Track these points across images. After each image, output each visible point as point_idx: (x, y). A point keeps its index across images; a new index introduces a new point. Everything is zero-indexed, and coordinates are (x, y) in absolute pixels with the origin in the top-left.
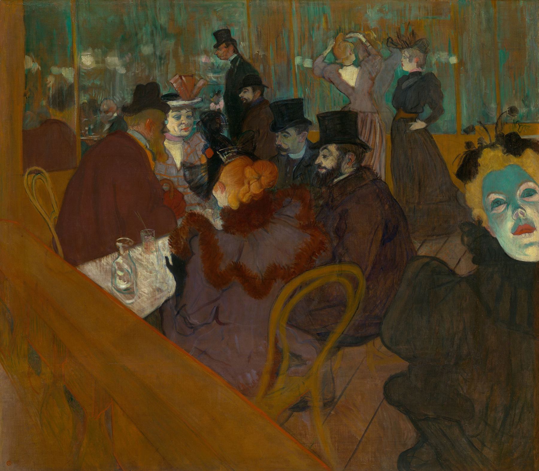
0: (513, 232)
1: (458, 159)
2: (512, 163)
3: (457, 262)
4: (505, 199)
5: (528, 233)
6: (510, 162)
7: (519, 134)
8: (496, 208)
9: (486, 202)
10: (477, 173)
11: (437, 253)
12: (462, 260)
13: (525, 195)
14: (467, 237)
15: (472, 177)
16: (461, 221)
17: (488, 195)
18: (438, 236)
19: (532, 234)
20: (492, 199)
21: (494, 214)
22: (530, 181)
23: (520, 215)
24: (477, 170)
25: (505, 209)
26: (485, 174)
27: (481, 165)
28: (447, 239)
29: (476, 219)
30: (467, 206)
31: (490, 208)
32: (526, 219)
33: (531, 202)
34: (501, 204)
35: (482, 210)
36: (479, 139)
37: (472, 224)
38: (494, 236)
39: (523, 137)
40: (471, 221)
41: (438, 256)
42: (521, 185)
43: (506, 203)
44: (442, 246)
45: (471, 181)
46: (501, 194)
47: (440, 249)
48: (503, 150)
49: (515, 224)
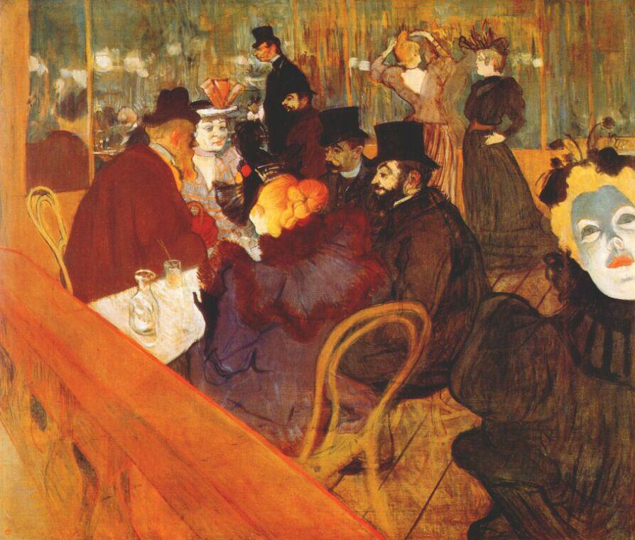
4: (598, 227)
8: (588, 237)
19: (630, 267)
20: (584, 226)
28: (529, 273)
45: (557, 205)
48: (596, 170)
49: (610, 255)
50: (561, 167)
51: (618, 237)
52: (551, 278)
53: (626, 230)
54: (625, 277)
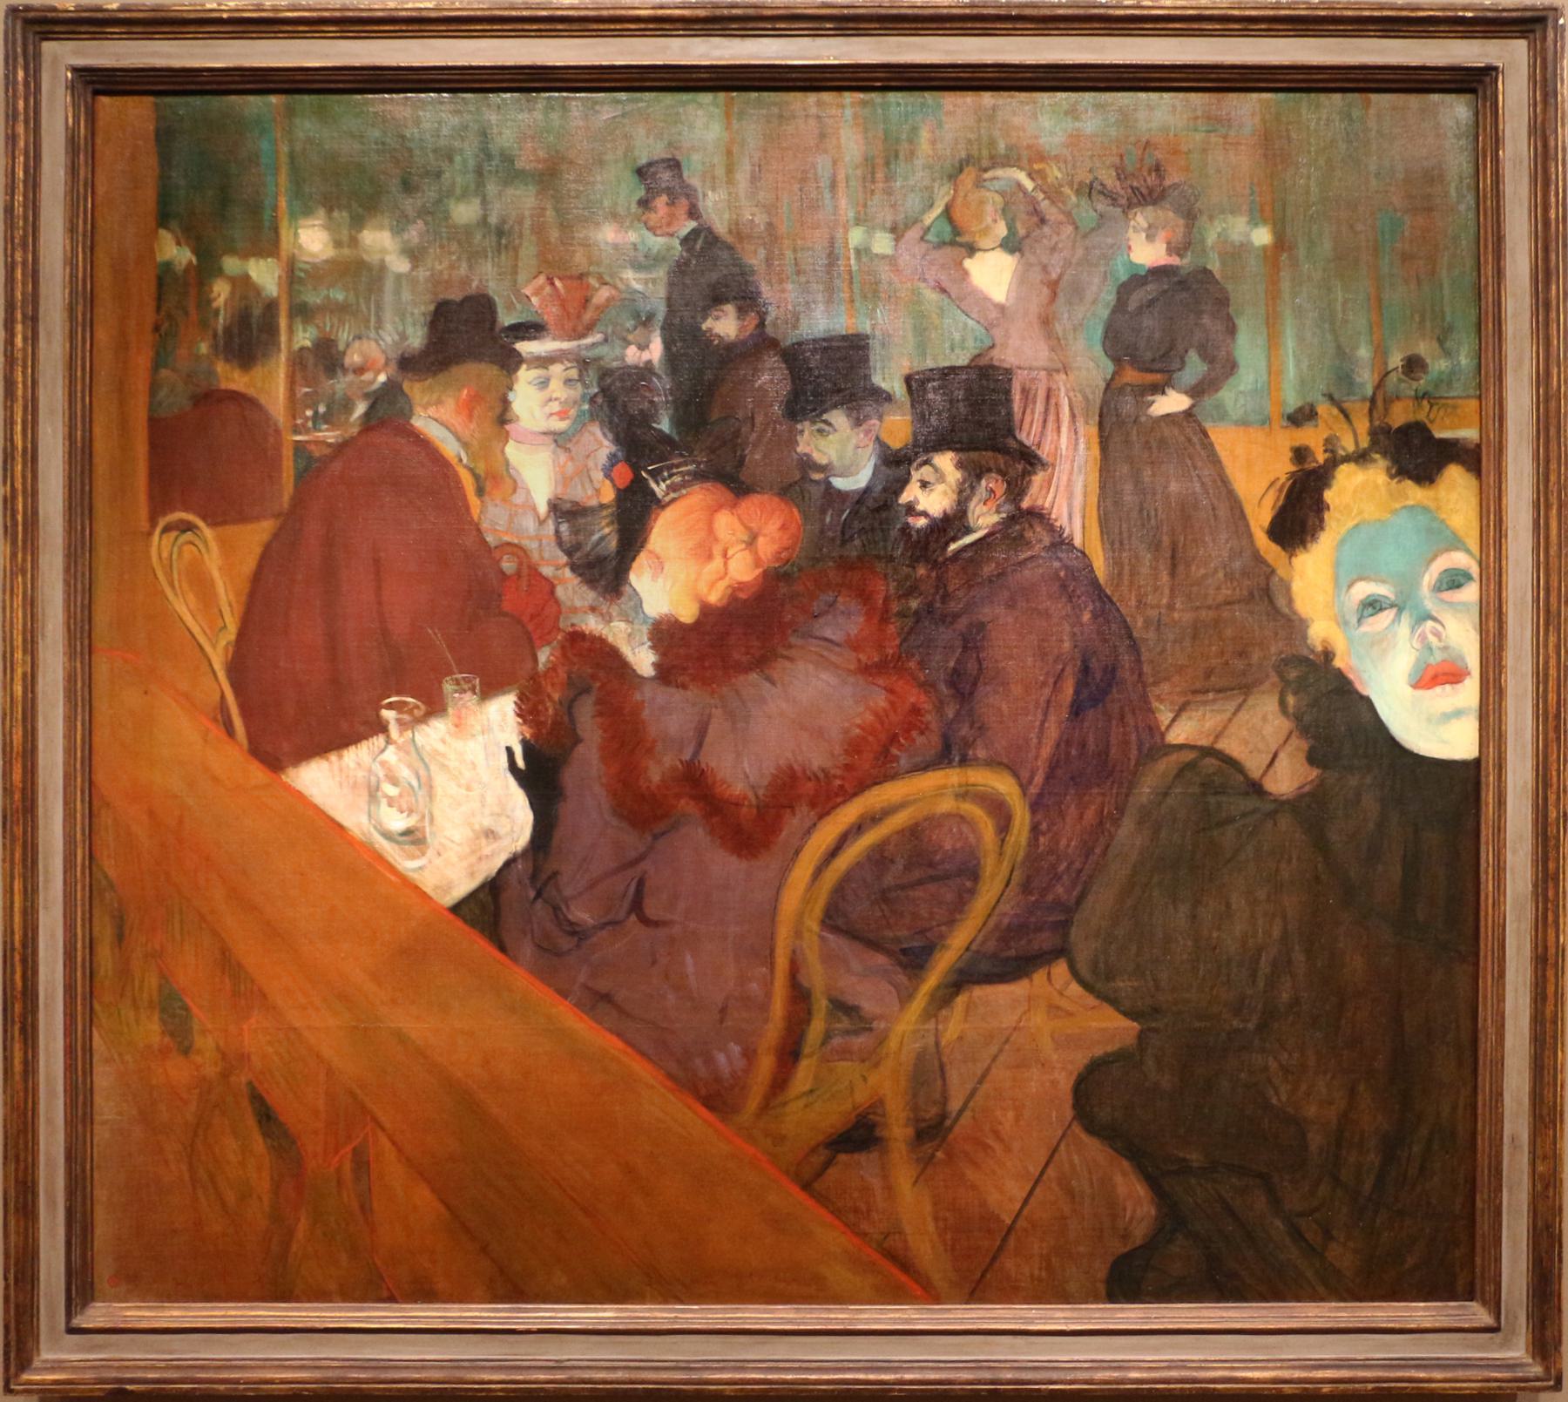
2: (1411, 502)
3: (1267, 762)
4: (1392, 597)
5: (1452, 683)
6: (1407, 498)
7: (1429, 425)
8: (1370, 620)
10: (1322, 529)
11: (1217, 737)
12: (1282, 755)
13: (1445, 586)
14: (1295, 693)
15: (1309, 538)
16: (1281, 652)
17: (1350, 586)
18: (1219, 691)
19: (1459, 686)
20: (1362, 596)
21: (1365, 634)
22: (1457, 549)
23: (1432, 639)
24: (1322, 520)
25: (1393, 621)
26: (1343, 531)
28: (1245, 701)
29: (1319, 648)
30: (1295, 613)
31: (1354, 620)
32: (1446, 648)
33: (1459, 603)
34: (1381, 609)
35: (1334, 626)
36: (1327, 441)
37: (1307, 659)
38: (1365, 693)
40: (1305, 652)
41: (1220, 746)
44: (1230, 720)
45: (1305, 547)
46: (1383, 582)
47: (1225, 728)
48: (1388, 470)
49: (1418, 660)
50: (1314, 465)
51: (1435, 619)
52: (1291, 710)
53: (1451, 604)
54: (1449, 710)
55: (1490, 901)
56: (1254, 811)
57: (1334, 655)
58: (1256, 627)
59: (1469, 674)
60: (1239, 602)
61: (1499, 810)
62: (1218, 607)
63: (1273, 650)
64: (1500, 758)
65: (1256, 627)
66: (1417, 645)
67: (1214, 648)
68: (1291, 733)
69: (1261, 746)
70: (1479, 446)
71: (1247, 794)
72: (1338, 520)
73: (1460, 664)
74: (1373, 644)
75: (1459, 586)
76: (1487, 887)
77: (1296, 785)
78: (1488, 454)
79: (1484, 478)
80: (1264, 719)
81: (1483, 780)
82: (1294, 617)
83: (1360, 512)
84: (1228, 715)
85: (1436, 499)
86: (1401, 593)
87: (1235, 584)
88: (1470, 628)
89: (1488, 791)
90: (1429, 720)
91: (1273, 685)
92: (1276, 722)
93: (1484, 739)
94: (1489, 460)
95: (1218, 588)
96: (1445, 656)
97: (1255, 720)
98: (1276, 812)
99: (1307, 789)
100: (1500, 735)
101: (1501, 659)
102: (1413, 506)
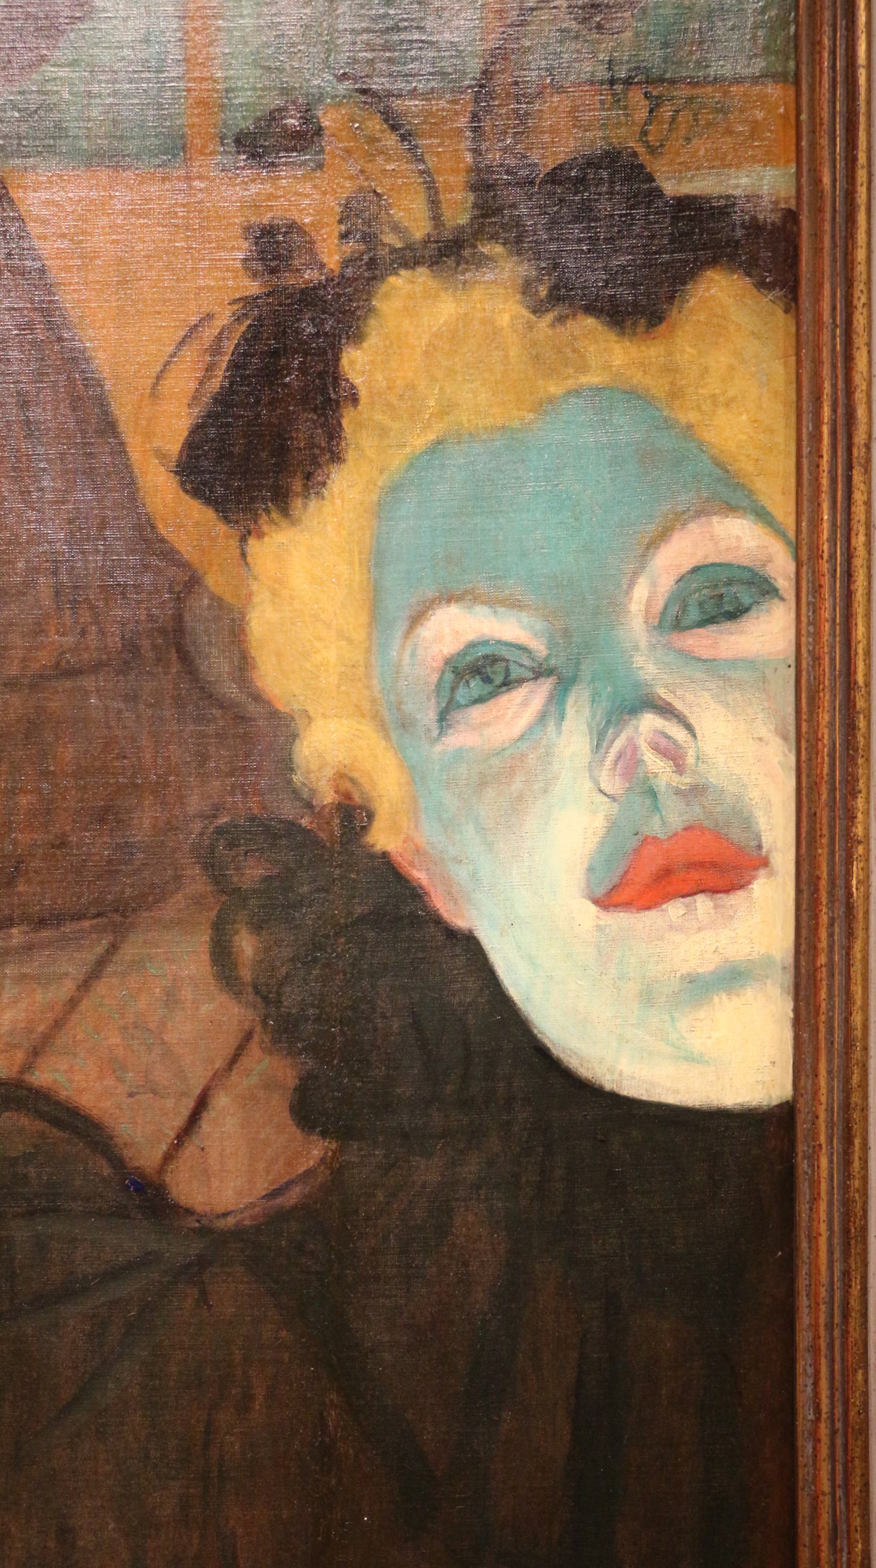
0: (600, 891)
1: (189, 354)
2: (593, 379)
3: (179, 1122)
4: (539, 647)
5: (714, 891)
6: (584, 368)
7: (644, 157)
8: (476, 713)
9: (398, 667)
10: (337, 458)
11: (36, 1052)
12: (221, 1101)
13: (694, 614)
14: (257, 927)
15: (297, 485)
16: (217, 809)
17: (417, 619)
18: (41, 923)
19: (736, 899)
20: (450, 647)
21: (459, 755)
22: (730, 509)
23: (654, 763)
24: (334, 433)
25: (542, 717)
26: (397, 461)
27: (363, 393)
28: (114, 948)
29: (327, 797)
30: (257, 697)
31: (428, 716)
32: (697, 791)
33: (734, 663)
34: (508, 684)
35: (368, 730)
36: (348, 213)
37: (292, 827)
38: (461, 923)
39: (670, 188)
40: (288, 810)
41: (41, 1077)
42: (663, 535)
43: (550, 672)
44: (73, 1004)
45: (285, 512)
46: (515, 605)
47: (58, 1024)
48: (527, 287)
49: (613, 827)
50: (310, 275)
51: (666, 710)
52: (246, 974)
53: (710, 665)
54: (707, 966)
55: (825, 1519)
56: (147, 1260)
57: (371, 816)
58: (145, 741)
59: (765, 863)
60: (96, 667)
61: (846, 1254)
62: (38, 682)
63: (195, 803)
64: (846, 1106)
65: (145, 741)
66: (612, 783)
67: (24, 800)
68: (248, 1036)
69: (162, 1076)
70: (792, 216)
71: (120, 1213)
72: (383, 432)
73: (736, 834)
74: (482, 784)
75: (736, 613)
76: (816, 1479)
77: (262, 1186)
78: (816, 235)
79: (805, 302)
80: (171, 999)
81: (803, 1166)
82: (253, 709)
83: (445, 410)
84: (68, 987)
85: (670, 369)
86: (566, 633)
87: (86, 617)
88: (765, 730)
89: (815, 1199)
90: (648, 997)
91: (198, 901)
92: (205, 1009)
93: (807, 1049)
94: (817, 251)
95: (39, 630)
96: (696, 812)
97: (142, 1004)
98: (202, 1262)
99: (293, 1196)
100: (848, 1043)
101: (851, 817)
102: (598, 390)
